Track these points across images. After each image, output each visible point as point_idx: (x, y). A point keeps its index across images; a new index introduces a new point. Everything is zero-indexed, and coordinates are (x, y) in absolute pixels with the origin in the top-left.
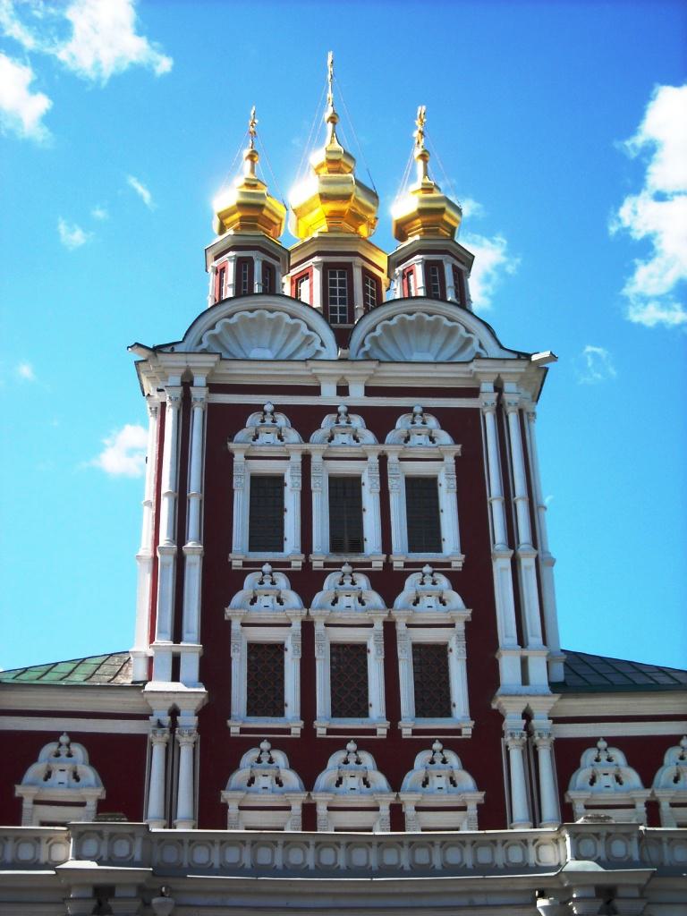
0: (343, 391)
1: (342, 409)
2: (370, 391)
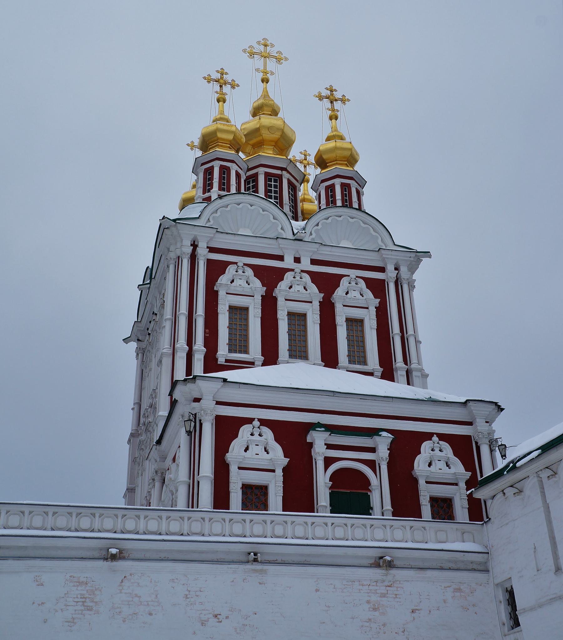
0: (297, 260)
1: (297, 270)
2: (314, 262)
